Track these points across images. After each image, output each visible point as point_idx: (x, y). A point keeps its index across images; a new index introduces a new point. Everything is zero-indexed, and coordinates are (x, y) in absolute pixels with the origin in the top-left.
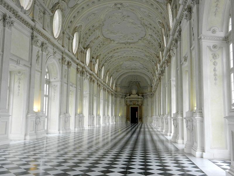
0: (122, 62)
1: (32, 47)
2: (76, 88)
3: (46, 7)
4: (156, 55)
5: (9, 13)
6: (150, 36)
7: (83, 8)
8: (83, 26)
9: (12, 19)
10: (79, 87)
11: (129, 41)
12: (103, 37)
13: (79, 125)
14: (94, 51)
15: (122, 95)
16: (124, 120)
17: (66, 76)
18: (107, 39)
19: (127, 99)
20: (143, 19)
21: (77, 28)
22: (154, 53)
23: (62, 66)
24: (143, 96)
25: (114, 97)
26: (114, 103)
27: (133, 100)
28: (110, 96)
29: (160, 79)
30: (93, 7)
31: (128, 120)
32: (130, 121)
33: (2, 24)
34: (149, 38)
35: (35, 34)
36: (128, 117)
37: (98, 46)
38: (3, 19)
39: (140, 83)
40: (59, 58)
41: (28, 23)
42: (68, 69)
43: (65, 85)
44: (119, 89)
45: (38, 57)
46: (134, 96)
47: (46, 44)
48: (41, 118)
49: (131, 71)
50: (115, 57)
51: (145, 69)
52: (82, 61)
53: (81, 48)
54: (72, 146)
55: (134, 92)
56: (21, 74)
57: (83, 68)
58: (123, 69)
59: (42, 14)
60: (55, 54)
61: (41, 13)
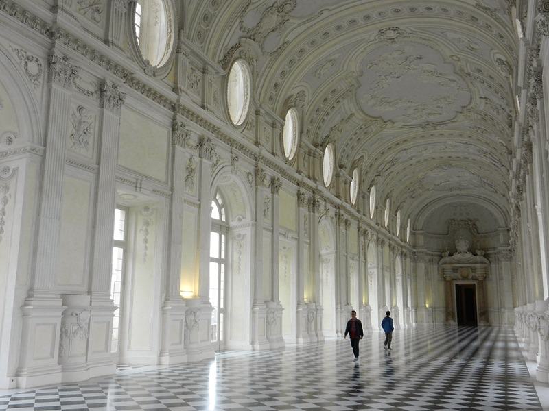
0: (422, 173)
1: (174, 149)
2: (298, 240)
3: (208, 59)
4: (506, 147)
5: (111, 78)
6: (483, 100)
7: (302, 50)
8: (307, 94)
9: (119, 90)
10: (305, 239)
11: (432, 118)
12: (363, 115)
13: (309, 330)
14: (344, 150)
16: (441, 317)
17: (269, 213)
18: (375, 119)
20: (459, 60)
21: (293, 99)
22: (500, 143)
23: (257, 189)
24: (486, 256)
25: (408, 259)
26: (411, 276)
28: (398, 259)
29: (518, 208)
30: (327, 46)
31: (450, 317)
32: (455, 321)
33: (97, 103)
34: (482, 106)
35: (181, 118)
36: (451, 309)
37: (354, 137)
38: (98, 92)
39: (477, 223)
40: (248, 171)
41: (161, 96)
42: (273, 196)
43: (266, 238)
44: (421, 240)
45: (191, 171)
46: (463, 256)
47: (209, 140)
49: (450, 193)
50: (403, 162)
51: (486, 186)
52: (311, 176)
53: (306, 145)
54: (293, 380)
55: (462, 245)
56: (150, 211)
57: (314, 192)
58: (428, 190)
59: (199, 74)
60: (236, 163)
61: (197, 72)
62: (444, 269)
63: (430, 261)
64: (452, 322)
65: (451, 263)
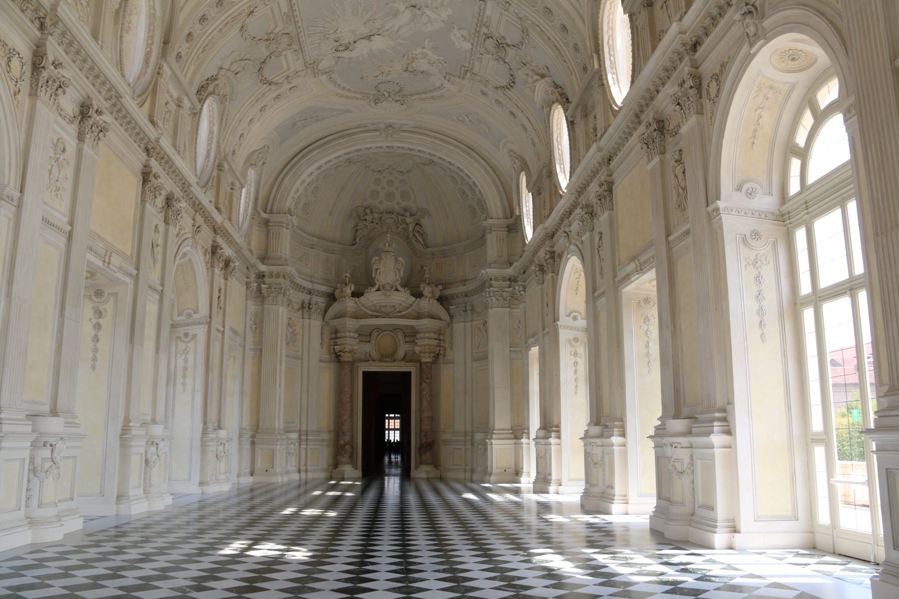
15: (310, 293)
16: (321, 455)
19: (341, 315)
24: (442, 300)
27: (379, 329)
31: (344, 459)
32: (357, 469)
36: (347, 438)
62: (336, 332)
63: (303, 307)
65: (356, 317)
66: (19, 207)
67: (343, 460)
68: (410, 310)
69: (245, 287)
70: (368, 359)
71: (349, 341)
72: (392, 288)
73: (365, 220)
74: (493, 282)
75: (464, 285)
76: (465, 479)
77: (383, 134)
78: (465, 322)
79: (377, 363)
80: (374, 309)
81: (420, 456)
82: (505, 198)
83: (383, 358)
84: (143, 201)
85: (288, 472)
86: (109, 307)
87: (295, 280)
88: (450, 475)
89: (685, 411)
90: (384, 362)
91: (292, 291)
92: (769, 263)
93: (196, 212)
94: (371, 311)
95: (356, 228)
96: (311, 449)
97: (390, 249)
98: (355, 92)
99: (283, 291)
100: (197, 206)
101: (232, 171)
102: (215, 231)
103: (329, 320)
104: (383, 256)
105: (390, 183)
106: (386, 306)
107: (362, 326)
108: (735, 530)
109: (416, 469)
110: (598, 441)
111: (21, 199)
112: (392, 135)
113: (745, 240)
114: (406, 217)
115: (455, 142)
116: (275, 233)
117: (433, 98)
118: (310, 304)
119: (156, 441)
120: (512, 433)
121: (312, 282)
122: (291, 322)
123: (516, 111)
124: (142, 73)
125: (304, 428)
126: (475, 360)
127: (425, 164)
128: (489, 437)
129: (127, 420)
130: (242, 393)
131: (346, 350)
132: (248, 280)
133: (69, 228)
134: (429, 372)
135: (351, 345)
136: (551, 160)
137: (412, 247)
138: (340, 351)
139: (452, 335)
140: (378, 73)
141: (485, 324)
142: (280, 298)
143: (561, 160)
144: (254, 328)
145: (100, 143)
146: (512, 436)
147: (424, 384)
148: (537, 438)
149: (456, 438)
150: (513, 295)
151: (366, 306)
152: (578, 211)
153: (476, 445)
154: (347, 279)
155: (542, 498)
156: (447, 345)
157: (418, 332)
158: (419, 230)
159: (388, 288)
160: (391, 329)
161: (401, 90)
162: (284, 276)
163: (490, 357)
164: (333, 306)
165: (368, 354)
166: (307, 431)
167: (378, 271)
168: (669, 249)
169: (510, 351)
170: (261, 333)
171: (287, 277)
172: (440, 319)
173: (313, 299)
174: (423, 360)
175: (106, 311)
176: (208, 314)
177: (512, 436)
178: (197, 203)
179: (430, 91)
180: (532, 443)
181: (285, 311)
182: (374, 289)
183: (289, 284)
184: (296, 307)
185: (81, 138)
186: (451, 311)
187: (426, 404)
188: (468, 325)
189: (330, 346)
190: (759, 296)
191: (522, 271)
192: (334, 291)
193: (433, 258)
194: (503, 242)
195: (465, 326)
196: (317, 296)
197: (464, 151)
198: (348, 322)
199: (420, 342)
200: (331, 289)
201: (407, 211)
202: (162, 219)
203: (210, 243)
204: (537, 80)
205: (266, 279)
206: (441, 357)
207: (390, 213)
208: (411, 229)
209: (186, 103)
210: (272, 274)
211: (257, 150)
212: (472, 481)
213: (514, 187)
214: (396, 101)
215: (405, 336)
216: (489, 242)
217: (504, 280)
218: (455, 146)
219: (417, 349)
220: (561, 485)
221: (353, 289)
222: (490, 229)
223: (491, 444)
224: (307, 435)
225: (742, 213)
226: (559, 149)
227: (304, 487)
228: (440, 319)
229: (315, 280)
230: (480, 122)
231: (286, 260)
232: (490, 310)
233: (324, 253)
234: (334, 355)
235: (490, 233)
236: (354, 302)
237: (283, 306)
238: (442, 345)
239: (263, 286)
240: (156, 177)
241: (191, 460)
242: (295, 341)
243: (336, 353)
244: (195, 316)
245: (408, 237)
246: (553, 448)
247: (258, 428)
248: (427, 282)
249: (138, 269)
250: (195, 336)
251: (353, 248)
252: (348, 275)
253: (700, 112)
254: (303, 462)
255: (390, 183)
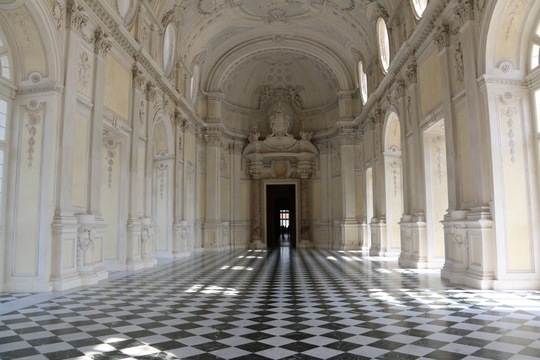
15: (234, 139)
16: (243, 235)
19: (252, 152)
24: (313, 141)
27: (275, 159)
31: (257, 237)
32: (264, 243)
36: (258, 224)
48: (92, 231)
62: (250, 161)
63: (230, 147)
64: (258, 243)
65: (261, 152)
66: (64, 94)
67: (256, 237)
68: (294, 147)
69: (195, 136)
70: (269, 177)
71: (257, 167)
72: (282, 134)
73: (265, 94)
74: (344, 129)
75: (326, 132)
76: (328, 248)
77: (274, 42)
78: (327, 154)
79: (275, 180)
80: (272, 147)
81: (302, 234)
82: (350, 78)
83: (278, 177)
84: (134, 87)
85: (223, 245)
86: (117, 151)
87: (225, 132)
88: (319, 246)
89: (463, 206)
90: (279, 179)
91: (223, 138)
92: (517, 113)
93: (165, 93)
94: (270, 148)
95: (260, 99)
96: (237, 231)
97: (280, 111)
98: (256, 16)
99: (217, 138)
100: (165, 89)
101: (185, 67)
102: (176, 104)
103: (246, 154)
104: (277, 115)
105: (280, 71)
106: (279, 145)
107: (265, 158)
108: (494, 278)
109: (299, 242)
110: (409, 225)
111: (64, 89)
112: (280, 42)
113: (501, 99)
114: (290, 91)
115: (318, 44)
116: (212, 104)
117: (304, 18)
118: (234, 145)
119: (147, 228)
120: (356, 220)
121: (234, 132)
122: (223, 156)
123: (355, 24)
124: (130, 11)
125: (232, 219)
126: (333, 177)
127: (300, 59)
128: (342, 223)
129: (130, 216)
130: (195, 199)
131: (256, 172)
132: (197, 132)
133: (92, 105)
134: (306, 184)
135: (259, 169)
136: (378, 53)
137: (294, 109)
138: (253, 173)
139: (319, 162)
140: (270, 4)
141: (339, 154)
142: (216, 142)
143: (384, 53)
144: (201, 161)
145: (107, 54)
146: (357, 222)
147: (303, 192)
148: (372, 223)
149: (323, 224)
150: (356, 137)
151: (268, 145)
152: (395, 84)
153: (335, 227)
154: (256, 130)
155: (375, 259)
156: (316, 168)
157: (299, 161)
158: (298, 99)
159: (280, 134)
160: (282, 159)
161: (284, 14)
162: (218, 129)
163: (342, 174)
164: (248, 146)
165: (269, 174)
166: (234, 221)
167: (274, 125)
168: (452, 106)
169: (355, 171)
170: (206, 164)
171: (219, 129)
172: (312, 152)
173: (235, 142)
174: (303, 177)
175: (115, 153)
176: (174, 153)
177: (357, 222)
178: (165, 87)
179: (302, 14)
180: (369, 226)
181: (219, 150)
182: (271, 136)
183: (221, 134)
184: (226, 147)
185: (96, 51)
186: (319, 147)
187: (304, 204)
188: (329, 155)
189: (246, 170)
190: (510, 133)
191: (361, 122)
192: (248, 137)
193: (307, 116)
194: (349, 105)
195: (327, 157)
196: (238, 140)
197: (324, 50)
198: (257, 156)
199: (300, 167)
200: (246, 136)
201: (291, 87)
202: (145, 98)
203: (174, 110)
204: (368, 4)
205: (207, 131)
206: (313, 175)
207: (280, 89)
208: (293, 98)
209: (156, 28)
210: (210, 128)
211: (199, 54)
212: (332, 249)
213: (355, 71)
214: (282, 21)
215: (291, 163)
216: (340, 104)
217: (350, 127)
218: (318, 47)
219: (298, 171)
220: (386, 251)
221: (259, 136)
222: (341, 97)
223: (344, 227)
224: (234, 223)
225: (500, 82)
226: (382, 46)
227: (233, 254)
228: (312, 152)
229: (237, 131)
230: (333, 31)
231: (219, 119)
232: (342, 146)
233: (241, 115)
234: (249, 176)
235: (341, 99)
236: (260, 143)
237: (218, 147)
238: (313, 168)
239: (205, 135)
240: (141, 73)
241: (167, 239)
242: (226, 168)
243: (250, 174)
244: (167, 154)
245: (291, 104)
246: (382, 229)
247: (206, 220)
248: (304, 130)
249: (132, 128)
250: (167, 166)
251: (258, 111)
252: (256, 127)
253: (472, 18)
254: (232, 239)
255: (280, 71)
